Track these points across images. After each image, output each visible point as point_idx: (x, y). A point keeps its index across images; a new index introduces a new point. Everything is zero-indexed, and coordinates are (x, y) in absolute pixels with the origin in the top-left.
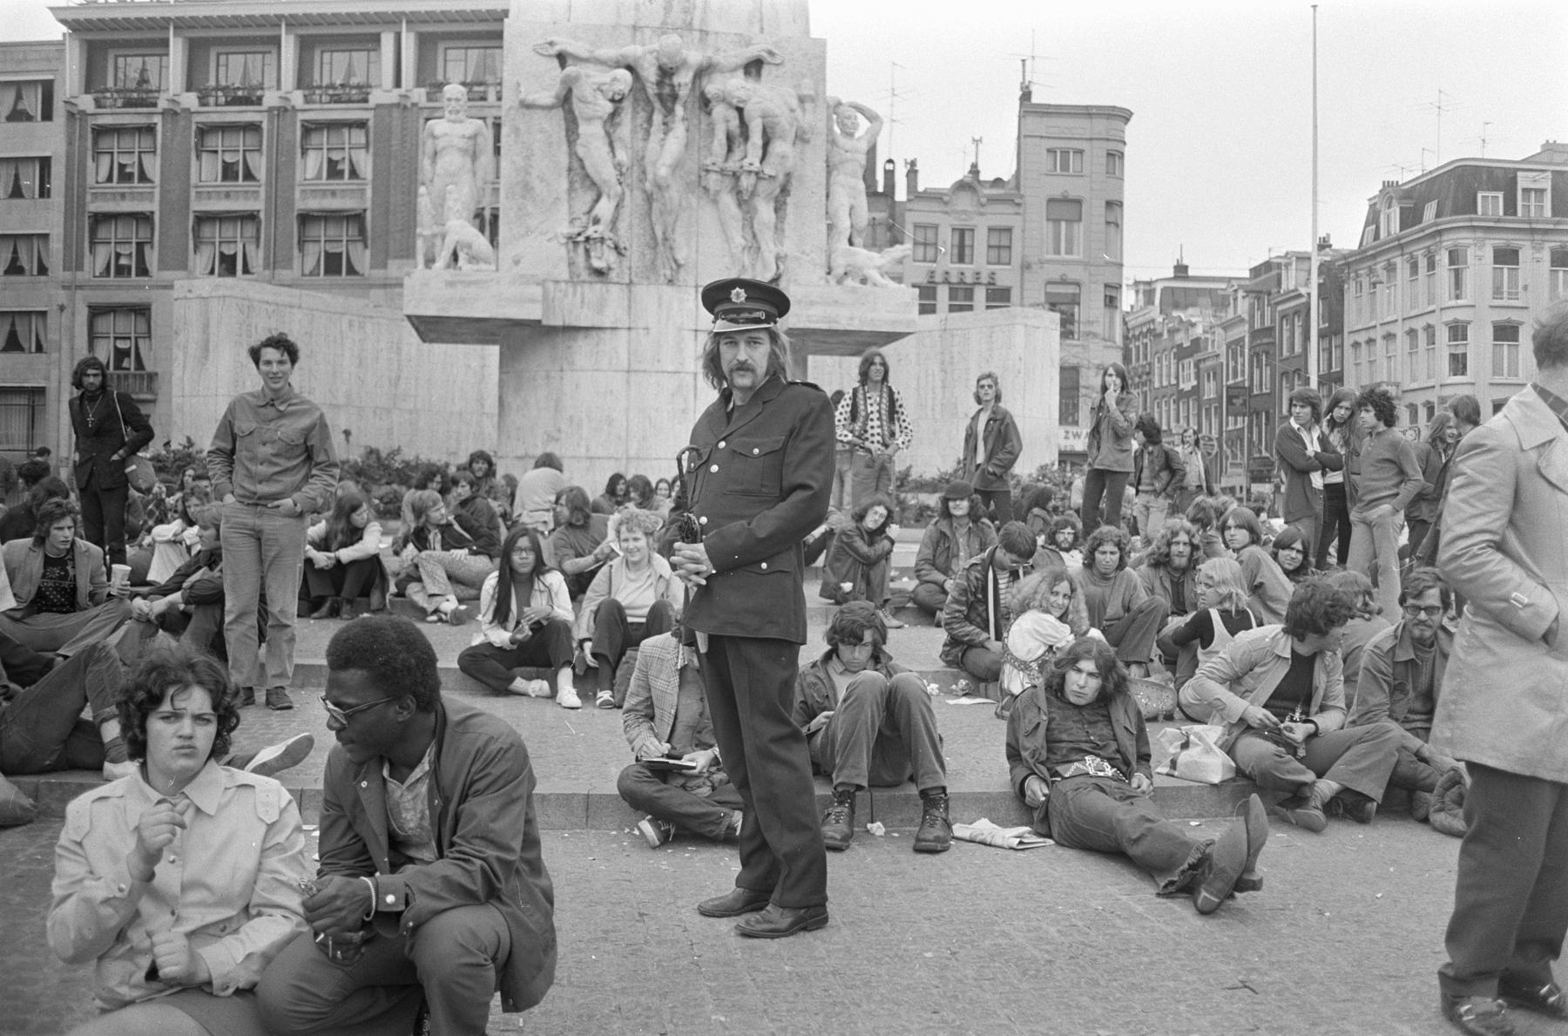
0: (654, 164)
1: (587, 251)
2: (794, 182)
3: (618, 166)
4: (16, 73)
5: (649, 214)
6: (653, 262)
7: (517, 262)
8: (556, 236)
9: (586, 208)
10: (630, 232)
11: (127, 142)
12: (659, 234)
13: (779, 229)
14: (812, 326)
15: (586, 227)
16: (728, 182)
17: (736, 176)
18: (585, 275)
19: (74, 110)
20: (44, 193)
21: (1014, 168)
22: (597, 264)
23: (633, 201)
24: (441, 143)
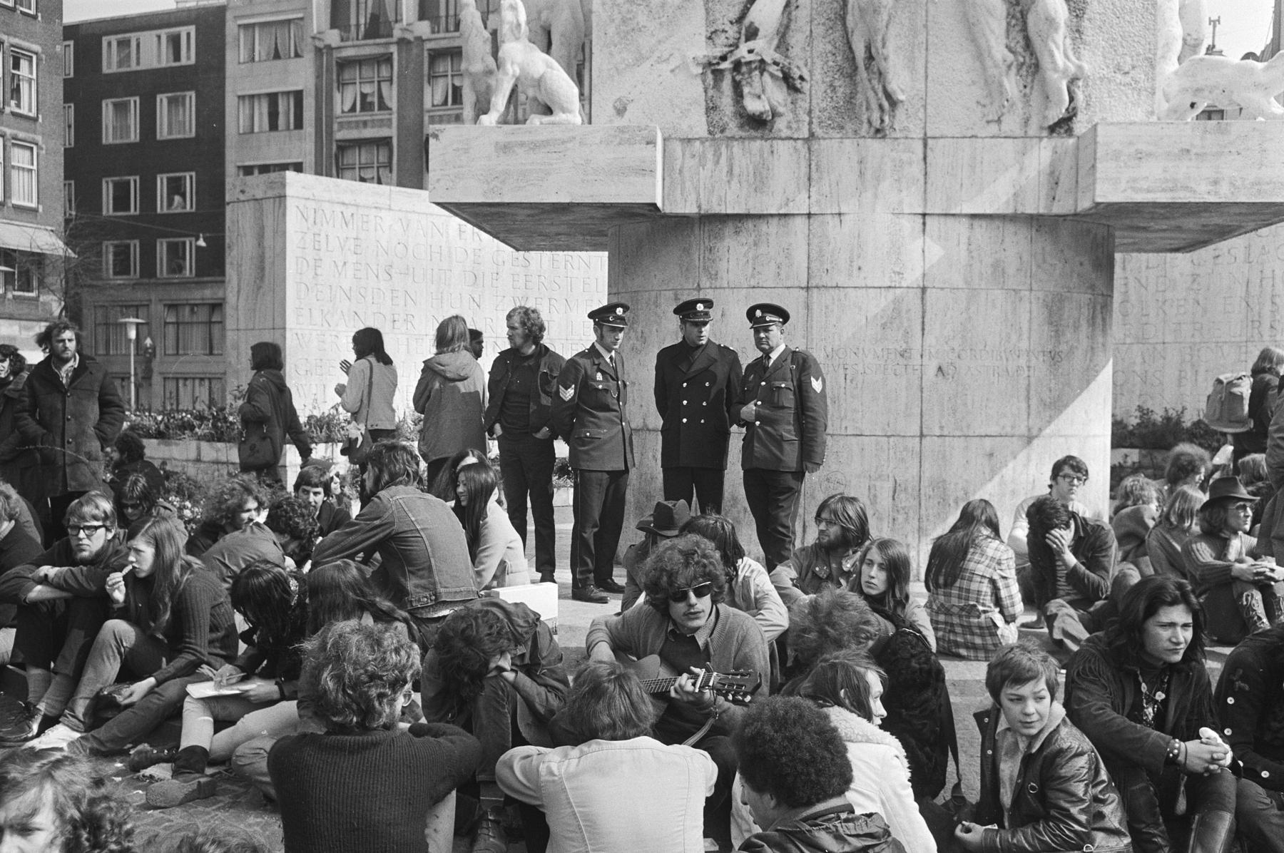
1: (737, 87)
4: (272, 13)
6: (850, 99)
7: (621, 111)
8: (683, 66)
9: (734, 13)
11: (367, 72)
12: (860, 53)
15: (736, 46)
18: (733, 128)
19: (320, 45)
20: (299, 124)
21: (1271, 36)
22: (753, 106)
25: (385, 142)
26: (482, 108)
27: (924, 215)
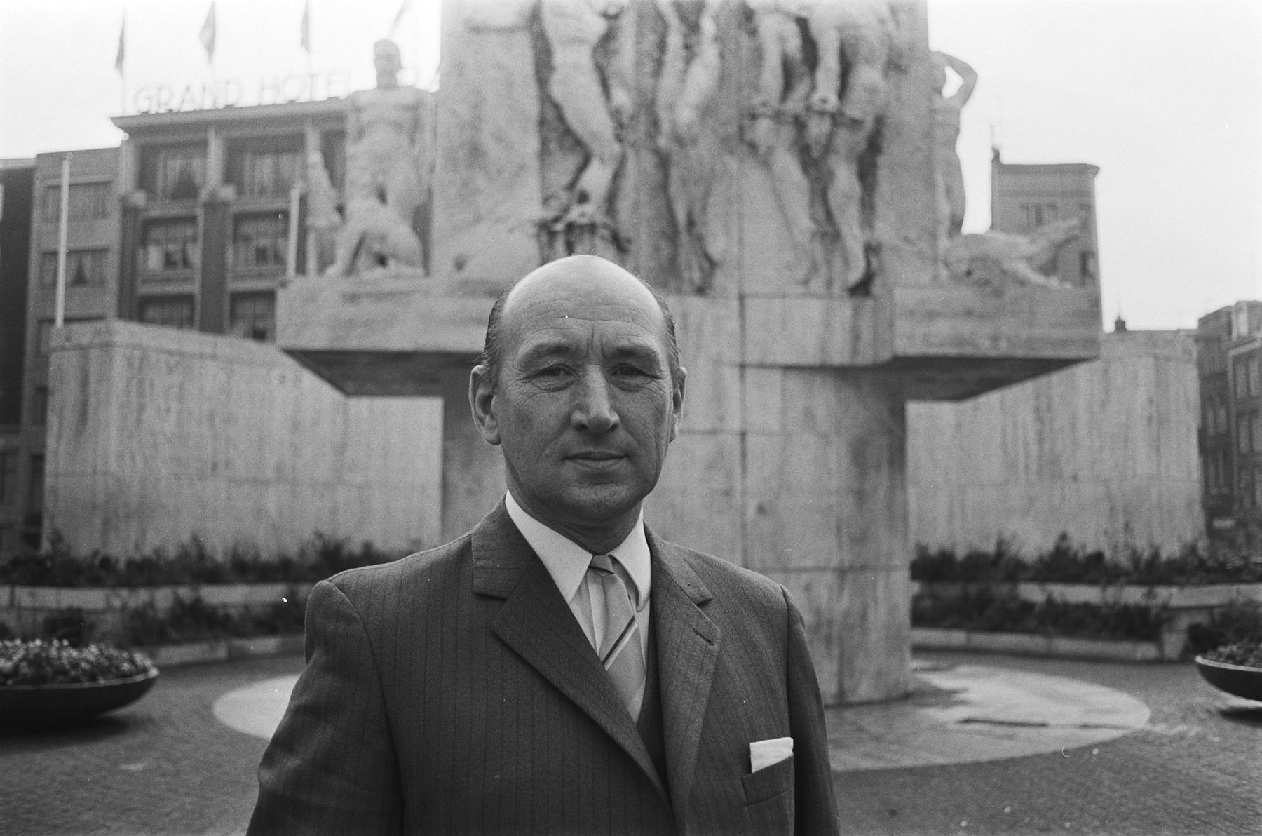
0: (671, 107)
2: (887, 133)
3: (616, 114)
5: (664, 186)
7: (460, 265)
9: (566, 179)
10: (636, 215)
12: (681, 217)
13: (867, 206)
14: (933, 351)
15: (566, 210)
16: (787, 133)
17: (799, 124)
23: (640, 167)
24: (365, 117)
25: (187, 299)
26: (325, 261)
27: (742, 366)
